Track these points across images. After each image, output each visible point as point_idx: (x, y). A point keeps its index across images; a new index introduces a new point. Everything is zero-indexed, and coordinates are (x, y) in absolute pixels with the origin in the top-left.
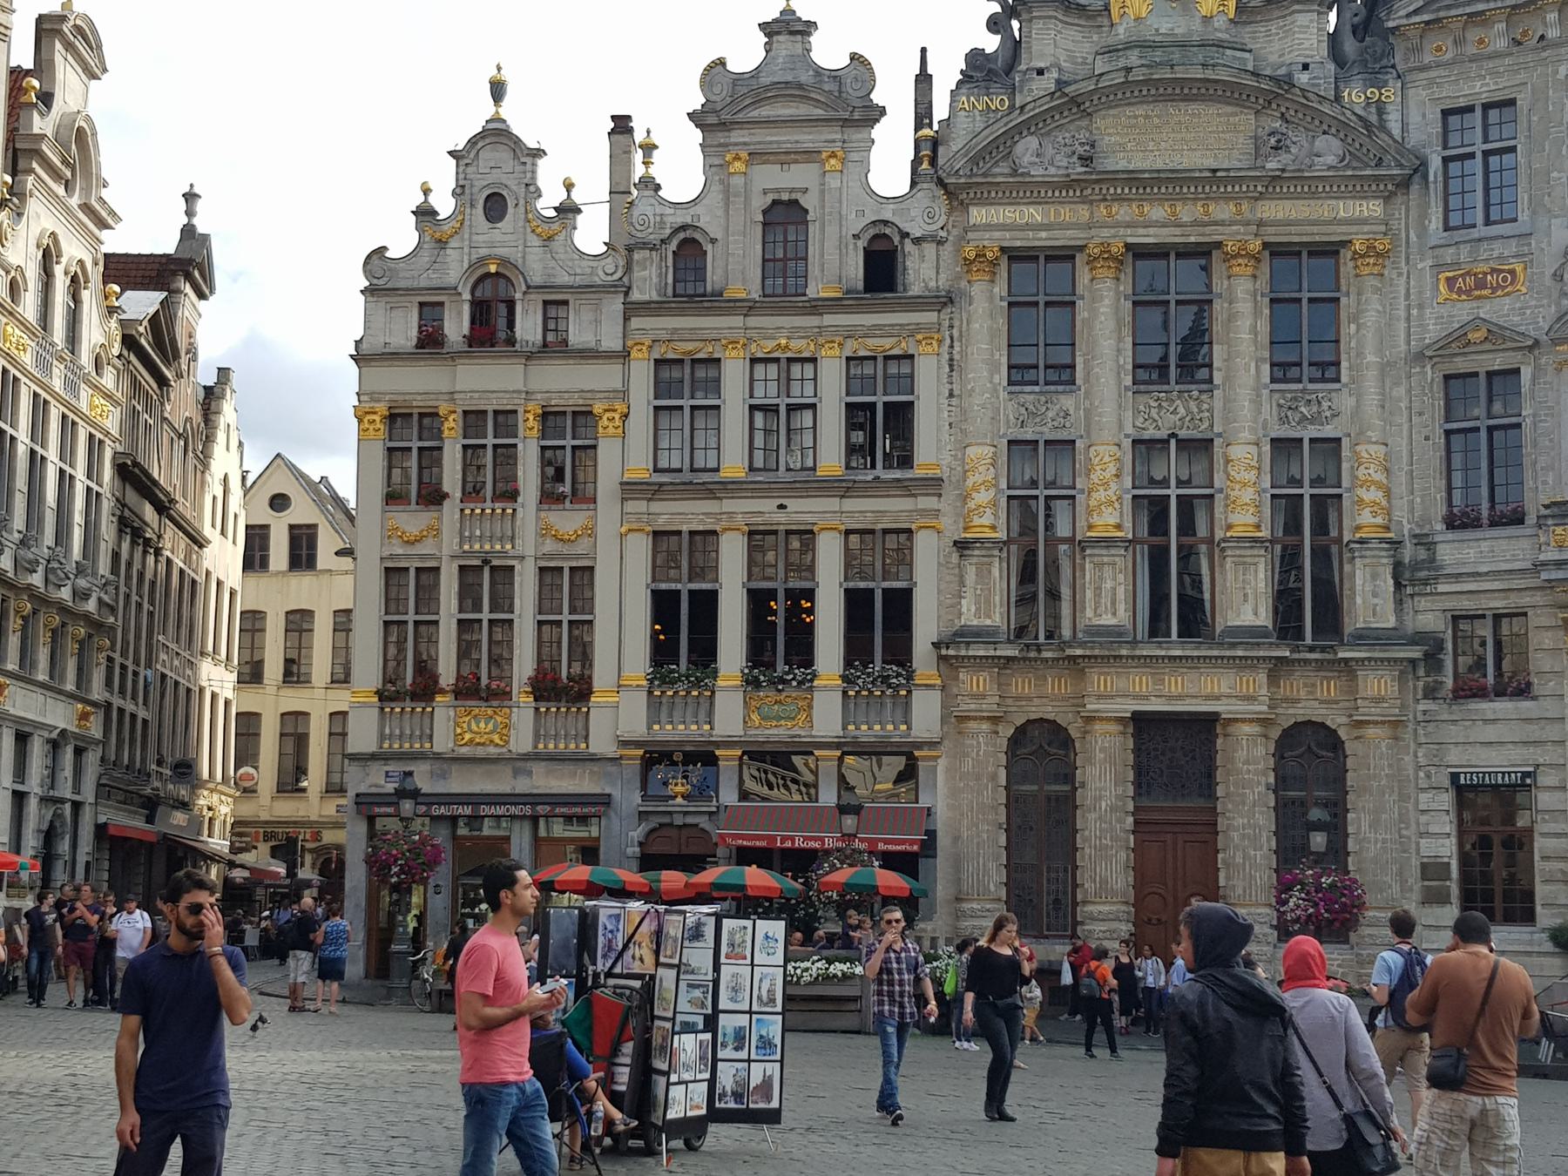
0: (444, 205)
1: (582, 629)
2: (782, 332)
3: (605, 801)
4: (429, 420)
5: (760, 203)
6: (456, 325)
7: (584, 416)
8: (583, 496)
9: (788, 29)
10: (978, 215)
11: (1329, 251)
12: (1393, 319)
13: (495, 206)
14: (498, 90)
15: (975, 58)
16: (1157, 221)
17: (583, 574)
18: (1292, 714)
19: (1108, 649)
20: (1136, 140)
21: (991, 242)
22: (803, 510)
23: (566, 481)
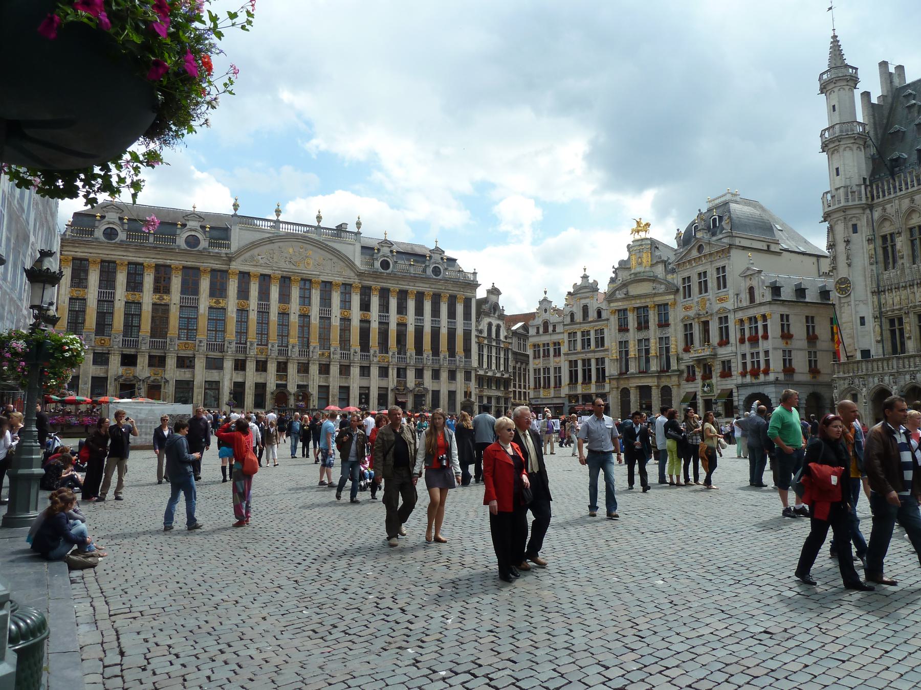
1: (560, 377)
4: (539, 346)
7: (559, 344)
8: (559, 355)
9: (585, 277)
10: (612, 305)
11: (667, 304)
12: (676, 316)
13: (546, 311)
15: (611, 278)
16: (638, 303)
17: (560, 368)
18: (662, 385)
19: (633, 376)
20: (634, 290)
22: (589, 356)
23: (557, 353)
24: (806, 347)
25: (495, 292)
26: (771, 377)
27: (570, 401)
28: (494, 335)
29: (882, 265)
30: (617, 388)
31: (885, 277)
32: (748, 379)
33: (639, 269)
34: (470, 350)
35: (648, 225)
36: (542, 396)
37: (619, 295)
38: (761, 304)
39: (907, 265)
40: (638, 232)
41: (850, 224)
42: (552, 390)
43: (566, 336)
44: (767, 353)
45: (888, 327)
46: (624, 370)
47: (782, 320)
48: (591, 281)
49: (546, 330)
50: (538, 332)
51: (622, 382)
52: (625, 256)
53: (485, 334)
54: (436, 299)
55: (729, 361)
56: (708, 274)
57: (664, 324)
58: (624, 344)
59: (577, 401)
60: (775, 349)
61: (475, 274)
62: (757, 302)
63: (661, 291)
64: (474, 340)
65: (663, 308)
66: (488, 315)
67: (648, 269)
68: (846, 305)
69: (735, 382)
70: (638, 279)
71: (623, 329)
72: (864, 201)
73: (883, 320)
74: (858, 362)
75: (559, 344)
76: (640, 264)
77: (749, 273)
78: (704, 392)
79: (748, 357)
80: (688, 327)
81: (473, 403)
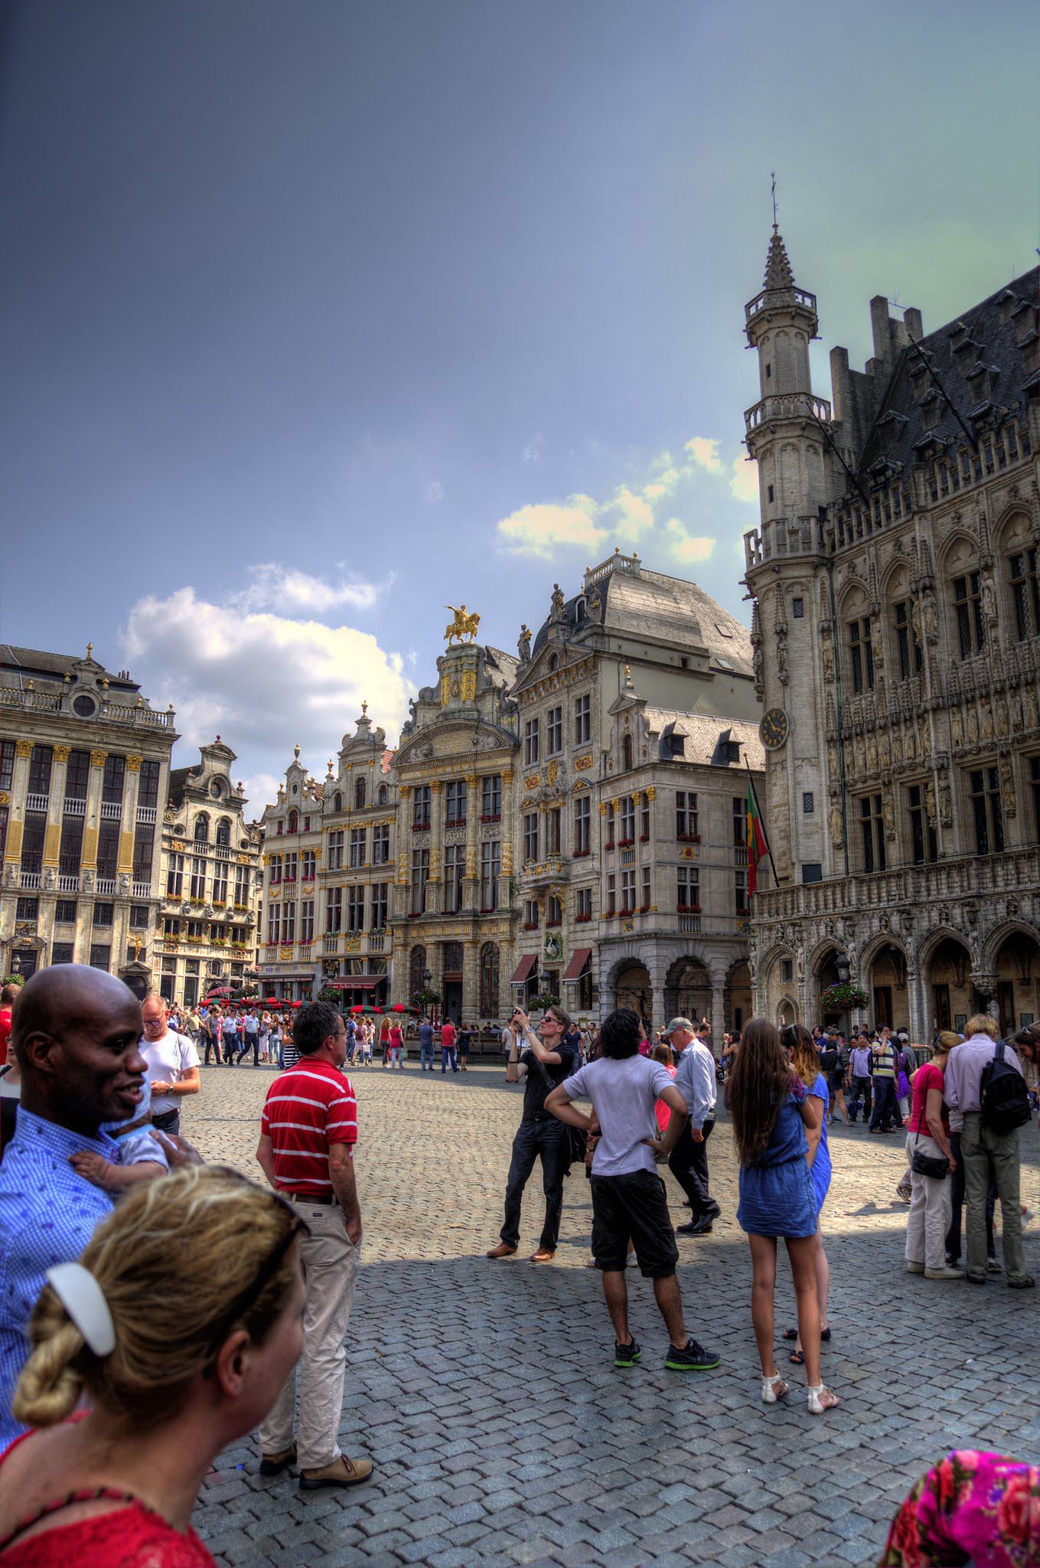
0: (284, 790)
1: (311, 920)
2: (358, 821)
3: (313, 976)
5: (355, 779)
6: (286, 827)
8: (313, 878)
9: (364, 722)
10: (404, 776)
11: (496, 777)
13: (295, 789)
14: (297, 753)
16: (448, 773)
17: (312, 903)
18: (483, 940)
20: (446, 746)
21: (406, 784)
22: (362, 879)
24: (733, 864)
25: (219, 751)
26: (651, 924)
27: (325, 971)
28: (212, 839)
29: (847, 684)
30: (405, 945)
31: (852, 708)
32: (616, 928)
33: (453, 706)
34: (149, 866)
35: (475, 618)
36: (278, 960)
37: (416, 756)
38: (641, 769)
39: (889, 681)
40: (458, 633)
41: (788, 599)
42: (296, 951)
43: (324, 839)
44: (646, 870)
45: (859, 816)
46: (418, 910)
47: (680, 802)
48: (373, 730)
49: (293, 830)
50: (279, 833)
51: (414, 933)
52: (432, 680)
53: (190, 835)
54: (79, 763)
55: (589, 891)
56: (564, 712)
57: (492, 817)
58: (422, 855)
59: (337, 970)
60: (660, 864)
61: (171, 714)
62: (635, 765)
63: (487, 749)
64: (160, 844)
65: (491, 782)
66: (200, 796)
67: (469, 704)
68: (779, 768)
69: (595, 935)
70: (449, 724)
71: (421, 826)
72: (814, 552)
73: (849, 800)
74: (793, 891)
75: (314, 857)
76: (456, 695)
77: (625, 705)
78: (548, 956)
79: (619, 882)
80: (531, 821)
81: (149, 972)
